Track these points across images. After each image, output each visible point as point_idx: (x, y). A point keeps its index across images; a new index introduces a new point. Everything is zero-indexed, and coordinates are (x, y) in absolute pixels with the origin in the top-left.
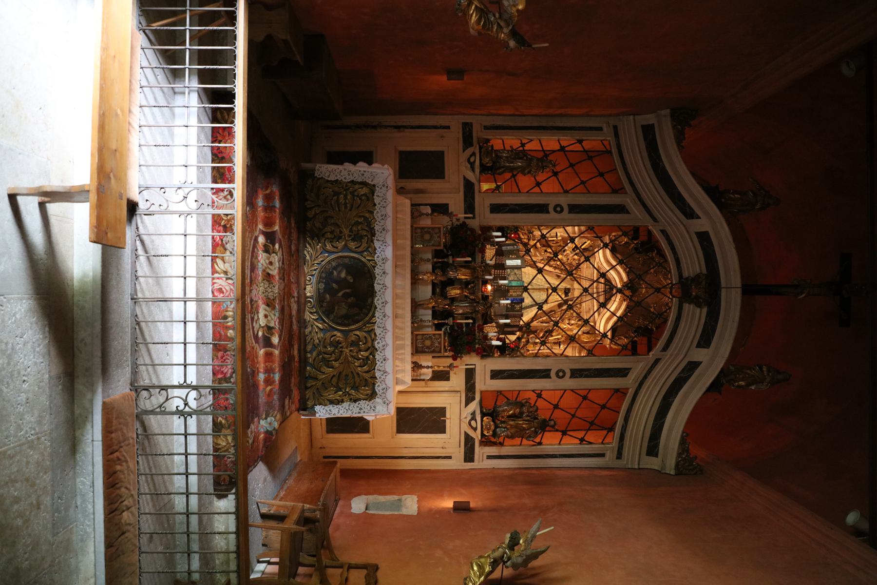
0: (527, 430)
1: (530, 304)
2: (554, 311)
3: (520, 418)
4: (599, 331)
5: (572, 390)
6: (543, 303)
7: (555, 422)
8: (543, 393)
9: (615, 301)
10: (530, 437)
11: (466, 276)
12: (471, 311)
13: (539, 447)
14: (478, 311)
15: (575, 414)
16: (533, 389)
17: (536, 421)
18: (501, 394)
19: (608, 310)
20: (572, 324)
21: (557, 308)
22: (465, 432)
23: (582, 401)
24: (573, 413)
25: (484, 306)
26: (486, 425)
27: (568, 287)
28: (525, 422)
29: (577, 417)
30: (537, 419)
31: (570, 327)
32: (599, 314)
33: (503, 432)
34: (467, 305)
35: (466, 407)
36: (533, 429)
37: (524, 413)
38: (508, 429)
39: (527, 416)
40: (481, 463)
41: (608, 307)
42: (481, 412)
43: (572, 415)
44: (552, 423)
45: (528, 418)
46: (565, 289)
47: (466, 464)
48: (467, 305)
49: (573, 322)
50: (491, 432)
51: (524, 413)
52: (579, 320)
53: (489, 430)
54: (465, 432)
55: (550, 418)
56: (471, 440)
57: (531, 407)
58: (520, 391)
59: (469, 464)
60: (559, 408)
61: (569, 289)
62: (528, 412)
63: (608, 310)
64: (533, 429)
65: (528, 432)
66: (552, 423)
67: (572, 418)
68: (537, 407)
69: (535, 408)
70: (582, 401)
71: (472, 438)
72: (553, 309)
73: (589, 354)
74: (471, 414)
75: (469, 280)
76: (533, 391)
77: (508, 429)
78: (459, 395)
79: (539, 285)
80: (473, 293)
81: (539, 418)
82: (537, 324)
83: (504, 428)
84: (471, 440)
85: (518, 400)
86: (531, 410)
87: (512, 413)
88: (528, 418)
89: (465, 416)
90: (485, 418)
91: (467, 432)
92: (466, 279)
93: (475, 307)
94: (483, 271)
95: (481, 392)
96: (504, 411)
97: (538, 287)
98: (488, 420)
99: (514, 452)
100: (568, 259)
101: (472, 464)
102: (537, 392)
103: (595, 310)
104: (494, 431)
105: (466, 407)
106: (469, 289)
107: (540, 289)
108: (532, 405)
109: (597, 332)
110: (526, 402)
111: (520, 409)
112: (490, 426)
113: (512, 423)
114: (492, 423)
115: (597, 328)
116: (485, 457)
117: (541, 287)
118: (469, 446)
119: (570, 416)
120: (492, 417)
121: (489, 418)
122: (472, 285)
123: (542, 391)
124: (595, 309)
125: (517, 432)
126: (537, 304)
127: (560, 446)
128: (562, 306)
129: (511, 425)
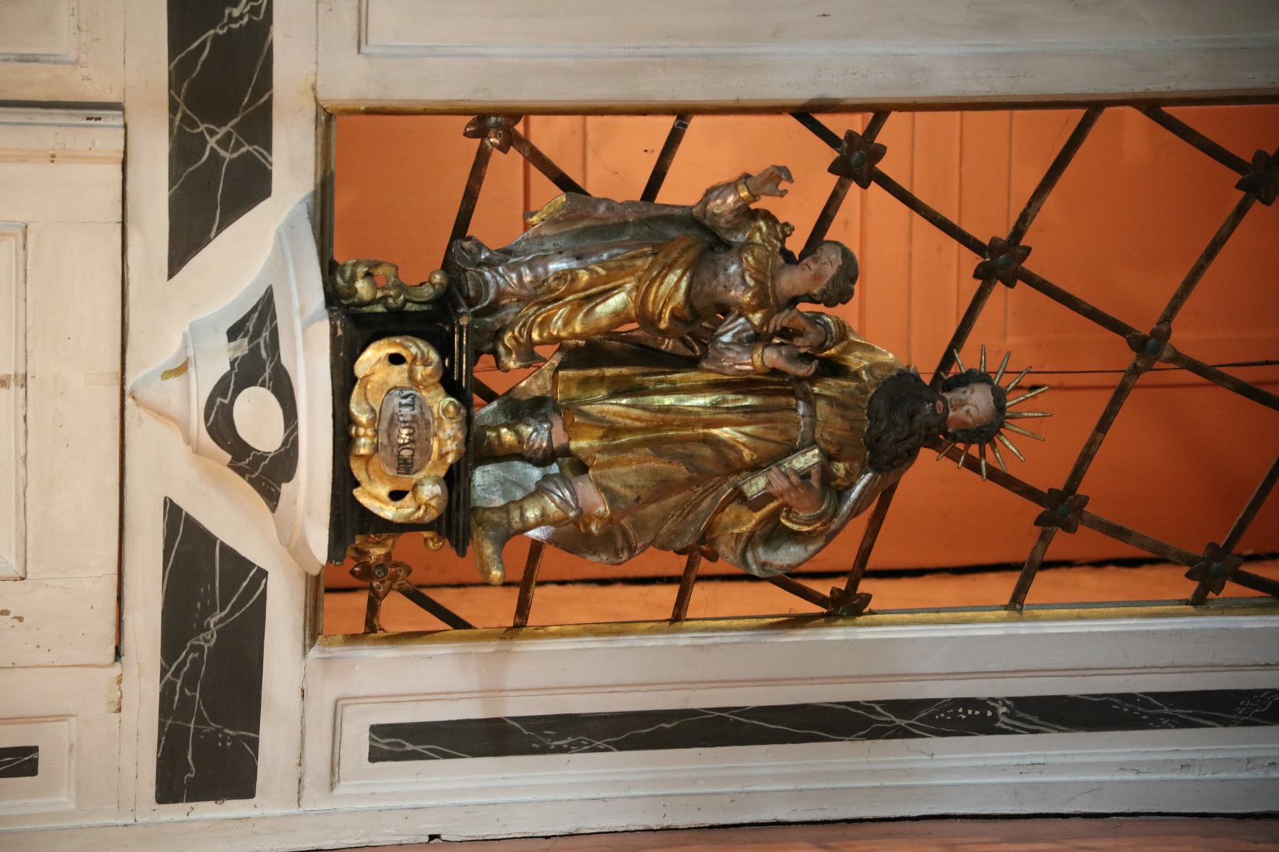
0: (755, 468)
3: (692, 363)
5: (1152, 107)
7: (999, 396)
8: (892, 132)
10: (773, 534)
13: (837, 634)
15: (1161, 335)
16: (803, 94)
17: (831, 387)
18: (511, 140)
22: (173, 512)
23: (1241, 211)
24: (1144, 329)
26: (383, 422)
28: (732, 400)
29: (1181, 361)
30: (834, 369)
33: (540, 490)
35: (177, 260)
36: (807, 459)
37: (725, 310)
38: (581, 467)
39: (758, 338)
40: (316, 801)
42: (334, 298)
43: (1139, 344)
44: (977, 401)
45: (772, 357)
47: (176, 812)
50: (431, 491)
51: (725, 310)
53: (406, 466)
54: (173, 512)
55: (948, 359)
56: (229, 588)
57: (788, 256)
58: (683, 114)
59: (206, 811)
60: (1031, 280)
62: (765, 299)
64: (807, 459)
65: (756, 486)
66: (977, 401)
67: (1135, 371)
68: (846, 254)
69: (829, 264)
70: (1241, 211)
71: (237, 564)
74: (233, 334)
76: (805, 114)
77: (581, 467)
78: (106, 137)
81: (856, 361)
83: (543, 459)
84: (229, 588)
85: (663, 197)
86: (791, 281)
87: (619, 317)
88: (772, 357)
89: (169, 354)
90: (372, 358)
91: (190, 506)
95: (327, 118)
96: (542, 295)
98: (397, 375)
99: (614, 687)
101: (234, 808)
102: (838, 124)
104: (455, 479)
105: (177, 260)
108: (796, 244)
110: (747, 214)
111: (694, 268)
112: (421, 426)
113: (617, 408)
114: (439, 401)
116: (357, 740)
118: (208, 640)
119: (1128, 357)
120: (445, 349)
121: (414, 348)
123: (880, 112)
125: (663, 488)
127: (1023, 628)
129: (612, 430)
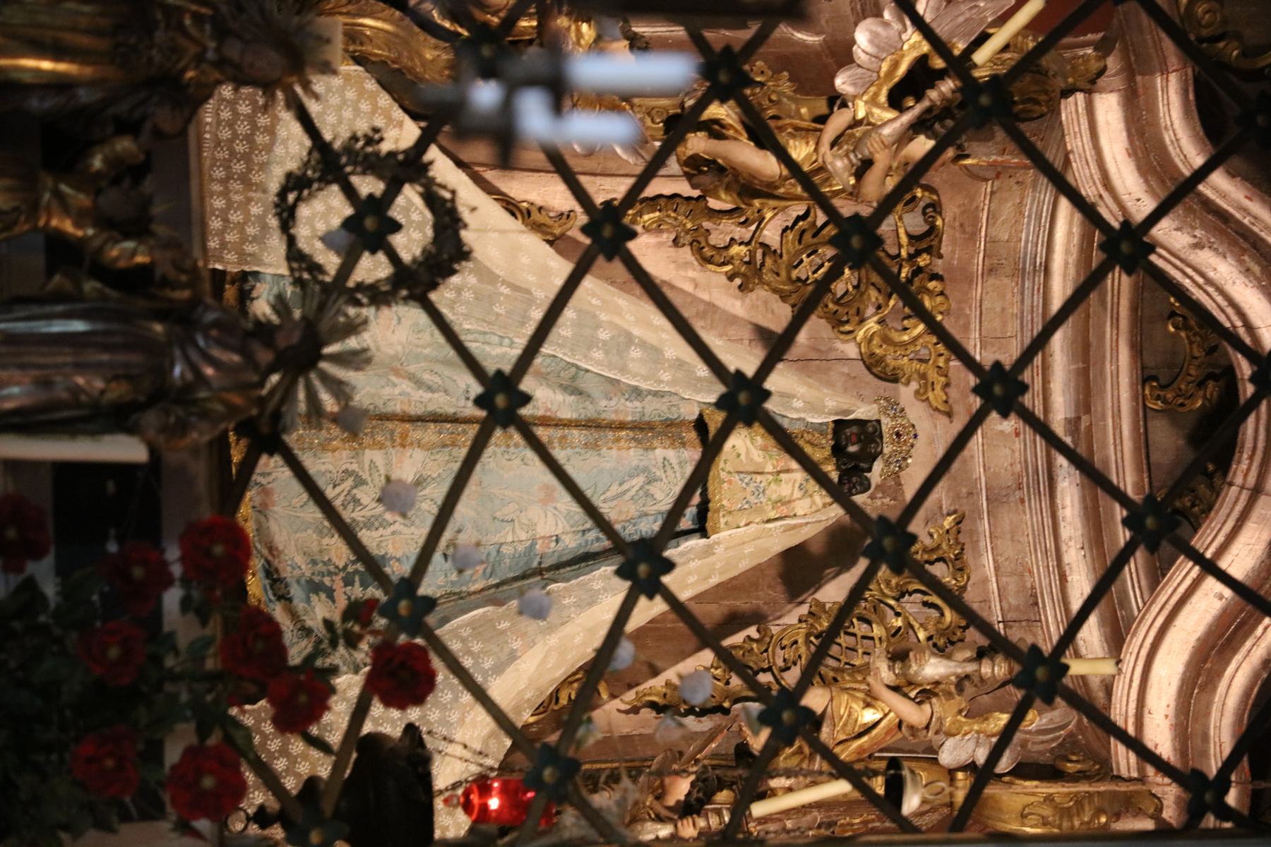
1: (571, 543)
2: (757, 618)
4: (1136, 744)
6: (670, 531)
9: (1257, 491)
11: (57, 53)
12: (118, 391)
14: (184, 396)
19: (1210, 568)
20: (927, 694)
21: (778, 593)
25: (243, 351)
27: (863, 411)
31: (914, 714)
32: (1116, 640)
34: (78, 326)
41: (1206, 542)
46: (840, 425)
48: (78, 326)
49: (933, 668)
52: (981, 654)
61: (868, 433)
63: (1210, 568)
72: (742, 604)
73: (1194, 810)
75: (84, 96)
79: (637, 393)
80: (137, 228)
82: (626, 725)
92: (59, 85)
93: (159, 354)
94: (222, 33)
97: (629, 410)
100: (867, 164)
103: (1076, 605)
106: (92, 184)
107: (643, 430)
109: (1124, 760)
115: (1122, 711)
117: (652, 409)
122: (124, 145)
124: (1081, 586)
126: (618, 545)
128: (816, 582)
